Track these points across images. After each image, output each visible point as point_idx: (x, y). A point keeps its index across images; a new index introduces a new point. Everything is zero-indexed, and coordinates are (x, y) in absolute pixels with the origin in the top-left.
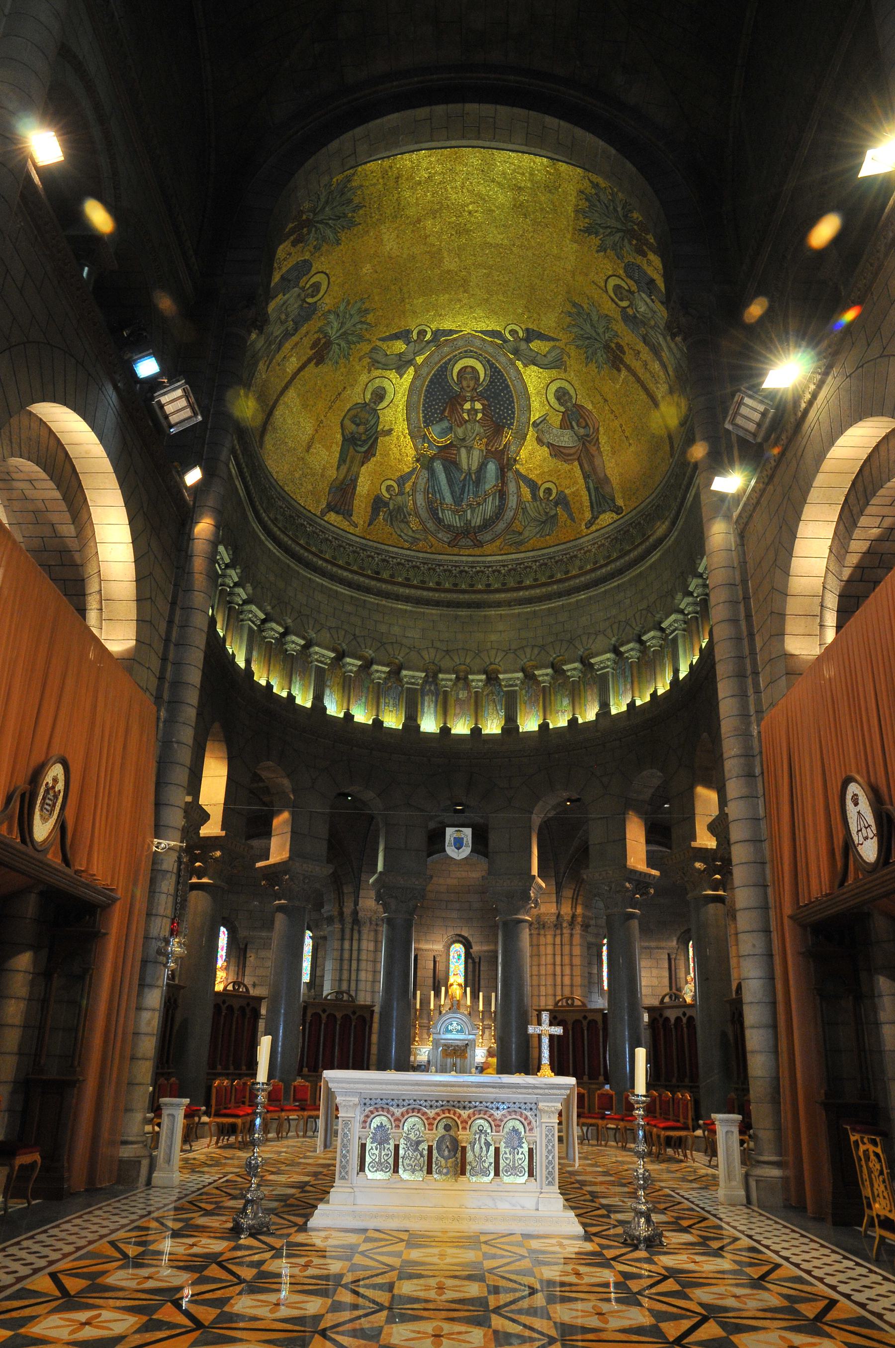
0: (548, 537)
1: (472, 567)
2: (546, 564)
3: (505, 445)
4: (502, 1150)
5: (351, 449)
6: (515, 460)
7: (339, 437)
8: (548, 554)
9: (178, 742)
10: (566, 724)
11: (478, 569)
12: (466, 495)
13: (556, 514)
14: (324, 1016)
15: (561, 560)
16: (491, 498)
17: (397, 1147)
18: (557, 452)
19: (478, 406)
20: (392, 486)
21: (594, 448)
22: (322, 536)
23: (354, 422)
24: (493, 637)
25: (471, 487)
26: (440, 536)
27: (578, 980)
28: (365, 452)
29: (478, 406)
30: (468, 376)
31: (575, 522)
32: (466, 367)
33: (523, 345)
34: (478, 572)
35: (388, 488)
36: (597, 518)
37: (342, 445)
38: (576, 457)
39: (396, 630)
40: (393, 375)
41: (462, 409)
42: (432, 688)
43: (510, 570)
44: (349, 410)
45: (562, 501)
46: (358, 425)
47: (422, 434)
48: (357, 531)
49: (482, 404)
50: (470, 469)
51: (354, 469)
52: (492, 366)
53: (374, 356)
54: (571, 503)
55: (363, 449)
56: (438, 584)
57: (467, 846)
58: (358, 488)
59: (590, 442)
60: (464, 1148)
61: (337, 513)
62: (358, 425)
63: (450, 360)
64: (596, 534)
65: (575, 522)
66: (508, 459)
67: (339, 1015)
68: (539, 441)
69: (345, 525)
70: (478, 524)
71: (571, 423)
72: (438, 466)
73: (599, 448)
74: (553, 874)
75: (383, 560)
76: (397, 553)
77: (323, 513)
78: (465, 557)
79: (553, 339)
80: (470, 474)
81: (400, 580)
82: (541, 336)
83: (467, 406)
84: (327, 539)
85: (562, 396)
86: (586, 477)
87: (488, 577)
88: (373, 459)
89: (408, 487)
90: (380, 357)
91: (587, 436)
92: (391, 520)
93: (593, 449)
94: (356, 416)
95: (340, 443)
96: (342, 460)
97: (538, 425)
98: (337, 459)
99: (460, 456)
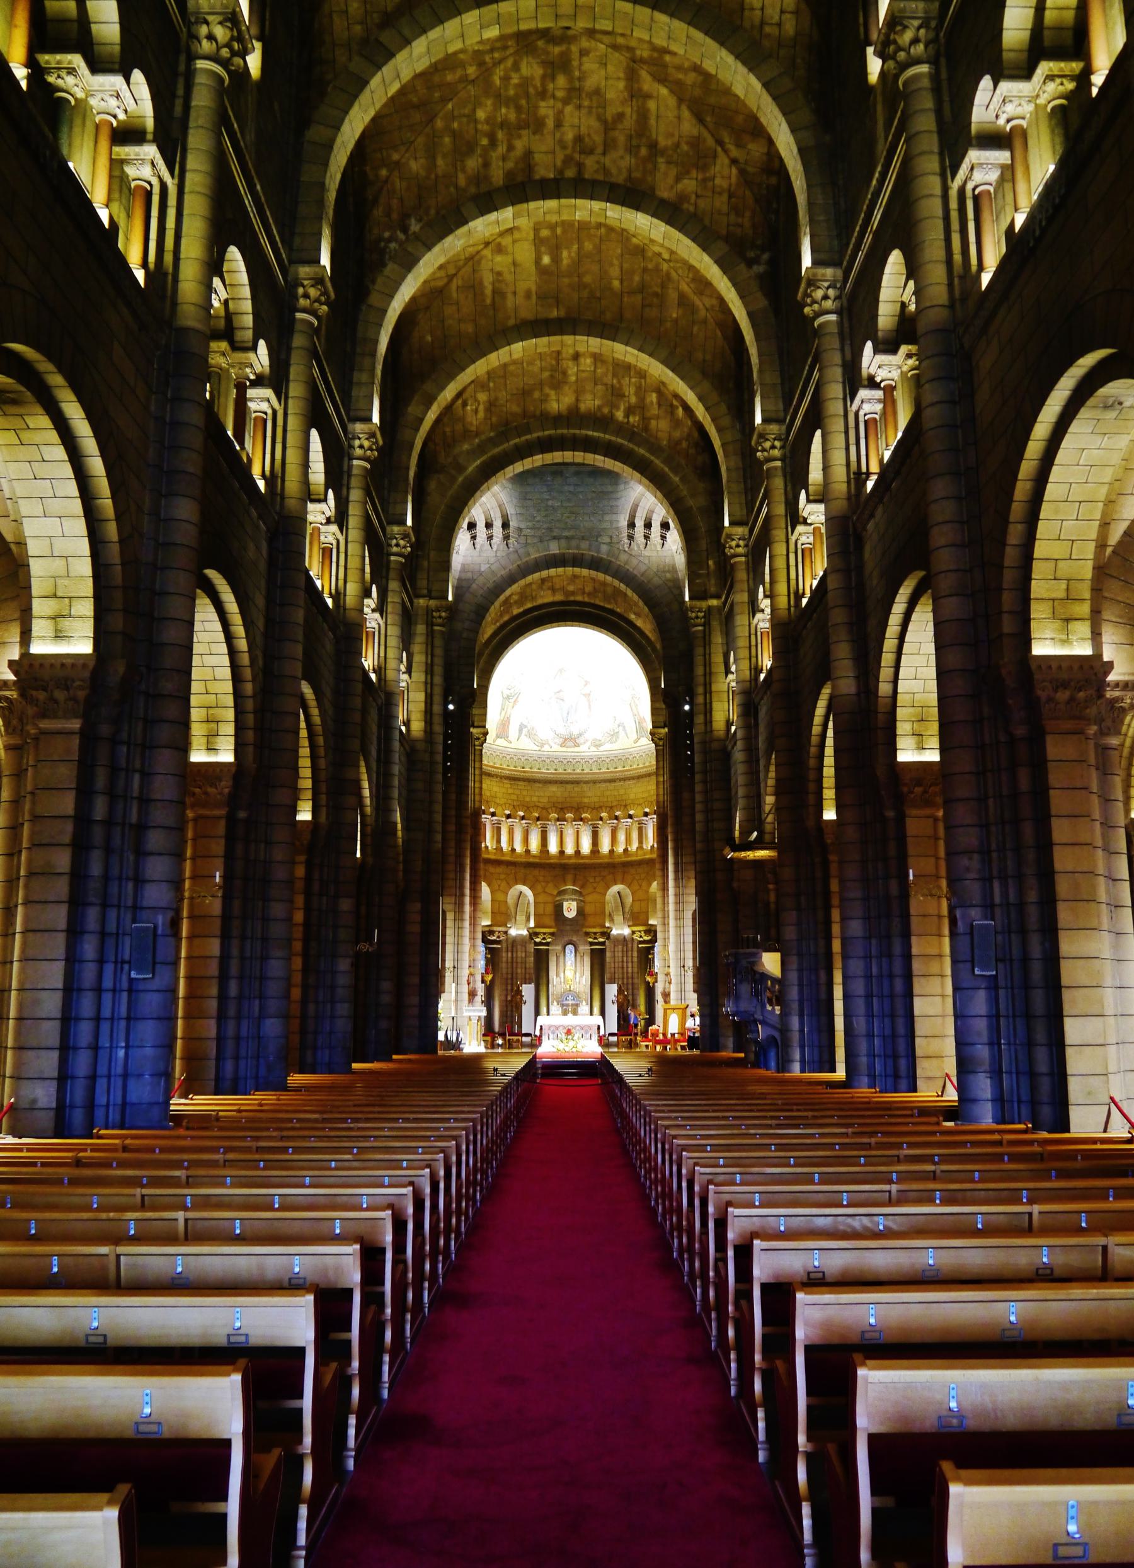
27: (636, 970)
39: (535, 799)
69: (505, 744)
78: (570, 751)
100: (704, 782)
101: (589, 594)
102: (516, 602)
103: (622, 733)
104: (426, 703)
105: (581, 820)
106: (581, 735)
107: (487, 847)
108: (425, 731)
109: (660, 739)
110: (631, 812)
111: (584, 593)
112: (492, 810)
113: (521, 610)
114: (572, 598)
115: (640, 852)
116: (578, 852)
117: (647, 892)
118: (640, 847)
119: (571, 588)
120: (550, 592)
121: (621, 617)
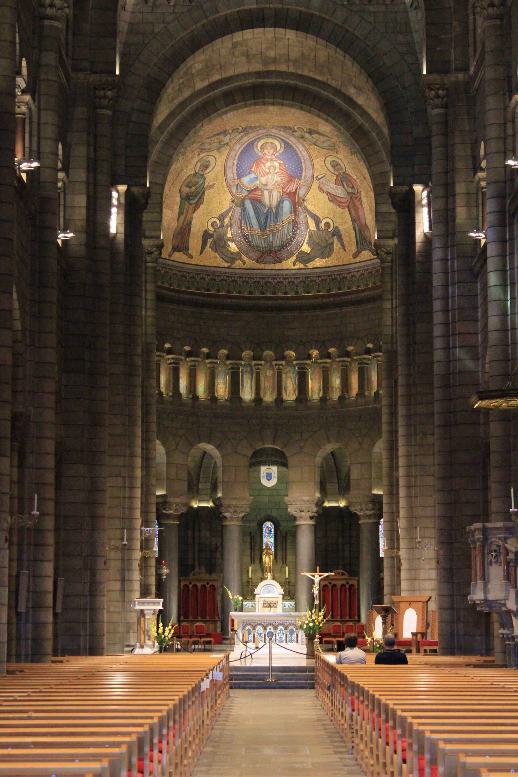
0: (327, 259)
1: (274, 279)
2: (325, 280)
3: (296, 189)
4: (288, 635)
5: (187, 203)
6: (304, 200)
7: (178, 199)
8: (327, 272)
9: (152, 485)
10: (337, 397)
11: (278, 280)
12: (268, 223)
13: (332, 244)
14: (190, 586)
15: (336, 279)
16: (287, 226)
17: (254, 635)
18: (333, 198)
19: (276, 164)
20: (215, 222)
21: (359, 203)
22: (171, 272)
23: (188, 186)
24: (290, 333)
25: (272, 217)
26: (250, 255)
28: (196, 203)
29: (276, 164)
30: (269, 147)
31: (345, 251)
32: (267, 143)
33: (307, 135)
34: (278, 282)
35: (213, 225)
36: (360, 252)
37: (181, 202)
38: (346, 205)
40: (215, 153)
41: (265, 166)
42: (249, 369)
43: (301, 282)
44: (185, 180)
45: (336, 233)
46: (190, 187)
47: (236, 183)
48: (193, 261)
49: (279, 163)
50: (271, 205)
51: (189, 216)
52: (286, 143)
53: (202, 147)
54: (343, 236)
55: (195, 201)
56: (250, 293)
57: (274, 478)
58: (192, 229)
59: (356, 198)
60: (276, 635)
61: (179, 251)
62: (190, 187)
63: (255, 140)
64: (359, 265)
65: (345, 251)
66: (299, 198)
67: (199, 585)
68: (320, 189)
70: (278, 245)
71: (343, 183)
72: (248, 205)
73: (361, 203)
74: (336, 481)
75: (212, 279)
76: (220, 272)
77: (170, 255)
79: (328, 137)
80: (271, 209)
81: (224, 293)
82: (318, 133)
83: (268, 164)
84: (174, 274)
85: (335, 165)
86: (353, 221)
87: (286, 287)
88: (202, 207)
89: (226, 221)
90: (207, 146)
91: (354, 194)
92: (216, 247)
93: (358, 204)
94: (189, 182)
95: (179, 202)
96: (181, 213)
97: (319, 179)
98: (177, 214)
99: (263, 196)
100: (446, 310)
101: (295, 61)
102: (200, 72)
103: (337, 245)
104: (88, 208)
105: (283, 358)
106: (283, 246)
107: (161, 394)
108: (87, 245)
109: (388, 253)
110: (350, 348)
111: (288, 60)
112: (167, 346)
113: (206, 83)
114: (272, 68)
115: (360, 401)
116: (279, 400)
117: (370, 452)
118: (361, 393)
119: (272, 54)
120: (243, 59)
121: (337, 92)
